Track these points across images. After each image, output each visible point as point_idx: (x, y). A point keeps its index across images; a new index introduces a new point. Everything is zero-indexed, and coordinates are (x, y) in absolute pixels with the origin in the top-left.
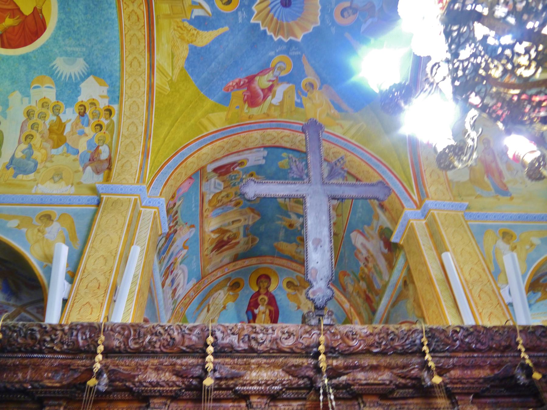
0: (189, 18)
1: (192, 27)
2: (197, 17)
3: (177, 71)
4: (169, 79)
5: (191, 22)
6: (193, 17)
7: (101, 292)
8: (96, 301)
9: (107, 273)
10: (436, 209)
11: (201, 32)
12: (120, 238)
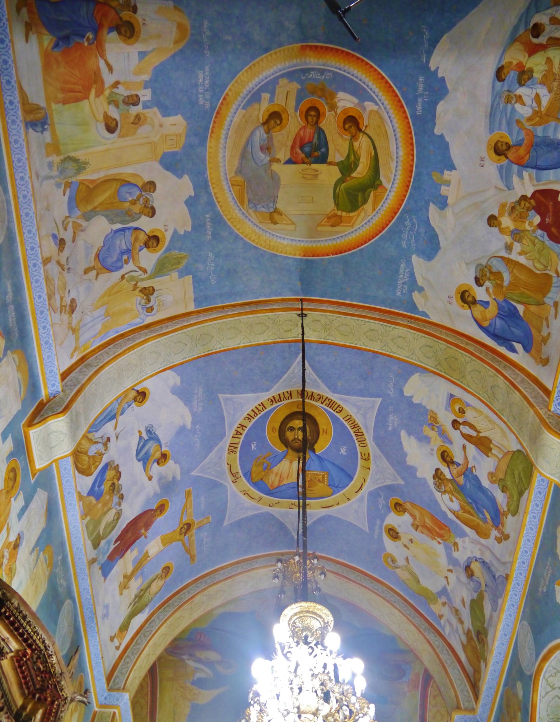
5: (193, 683)
6: (195, 679)
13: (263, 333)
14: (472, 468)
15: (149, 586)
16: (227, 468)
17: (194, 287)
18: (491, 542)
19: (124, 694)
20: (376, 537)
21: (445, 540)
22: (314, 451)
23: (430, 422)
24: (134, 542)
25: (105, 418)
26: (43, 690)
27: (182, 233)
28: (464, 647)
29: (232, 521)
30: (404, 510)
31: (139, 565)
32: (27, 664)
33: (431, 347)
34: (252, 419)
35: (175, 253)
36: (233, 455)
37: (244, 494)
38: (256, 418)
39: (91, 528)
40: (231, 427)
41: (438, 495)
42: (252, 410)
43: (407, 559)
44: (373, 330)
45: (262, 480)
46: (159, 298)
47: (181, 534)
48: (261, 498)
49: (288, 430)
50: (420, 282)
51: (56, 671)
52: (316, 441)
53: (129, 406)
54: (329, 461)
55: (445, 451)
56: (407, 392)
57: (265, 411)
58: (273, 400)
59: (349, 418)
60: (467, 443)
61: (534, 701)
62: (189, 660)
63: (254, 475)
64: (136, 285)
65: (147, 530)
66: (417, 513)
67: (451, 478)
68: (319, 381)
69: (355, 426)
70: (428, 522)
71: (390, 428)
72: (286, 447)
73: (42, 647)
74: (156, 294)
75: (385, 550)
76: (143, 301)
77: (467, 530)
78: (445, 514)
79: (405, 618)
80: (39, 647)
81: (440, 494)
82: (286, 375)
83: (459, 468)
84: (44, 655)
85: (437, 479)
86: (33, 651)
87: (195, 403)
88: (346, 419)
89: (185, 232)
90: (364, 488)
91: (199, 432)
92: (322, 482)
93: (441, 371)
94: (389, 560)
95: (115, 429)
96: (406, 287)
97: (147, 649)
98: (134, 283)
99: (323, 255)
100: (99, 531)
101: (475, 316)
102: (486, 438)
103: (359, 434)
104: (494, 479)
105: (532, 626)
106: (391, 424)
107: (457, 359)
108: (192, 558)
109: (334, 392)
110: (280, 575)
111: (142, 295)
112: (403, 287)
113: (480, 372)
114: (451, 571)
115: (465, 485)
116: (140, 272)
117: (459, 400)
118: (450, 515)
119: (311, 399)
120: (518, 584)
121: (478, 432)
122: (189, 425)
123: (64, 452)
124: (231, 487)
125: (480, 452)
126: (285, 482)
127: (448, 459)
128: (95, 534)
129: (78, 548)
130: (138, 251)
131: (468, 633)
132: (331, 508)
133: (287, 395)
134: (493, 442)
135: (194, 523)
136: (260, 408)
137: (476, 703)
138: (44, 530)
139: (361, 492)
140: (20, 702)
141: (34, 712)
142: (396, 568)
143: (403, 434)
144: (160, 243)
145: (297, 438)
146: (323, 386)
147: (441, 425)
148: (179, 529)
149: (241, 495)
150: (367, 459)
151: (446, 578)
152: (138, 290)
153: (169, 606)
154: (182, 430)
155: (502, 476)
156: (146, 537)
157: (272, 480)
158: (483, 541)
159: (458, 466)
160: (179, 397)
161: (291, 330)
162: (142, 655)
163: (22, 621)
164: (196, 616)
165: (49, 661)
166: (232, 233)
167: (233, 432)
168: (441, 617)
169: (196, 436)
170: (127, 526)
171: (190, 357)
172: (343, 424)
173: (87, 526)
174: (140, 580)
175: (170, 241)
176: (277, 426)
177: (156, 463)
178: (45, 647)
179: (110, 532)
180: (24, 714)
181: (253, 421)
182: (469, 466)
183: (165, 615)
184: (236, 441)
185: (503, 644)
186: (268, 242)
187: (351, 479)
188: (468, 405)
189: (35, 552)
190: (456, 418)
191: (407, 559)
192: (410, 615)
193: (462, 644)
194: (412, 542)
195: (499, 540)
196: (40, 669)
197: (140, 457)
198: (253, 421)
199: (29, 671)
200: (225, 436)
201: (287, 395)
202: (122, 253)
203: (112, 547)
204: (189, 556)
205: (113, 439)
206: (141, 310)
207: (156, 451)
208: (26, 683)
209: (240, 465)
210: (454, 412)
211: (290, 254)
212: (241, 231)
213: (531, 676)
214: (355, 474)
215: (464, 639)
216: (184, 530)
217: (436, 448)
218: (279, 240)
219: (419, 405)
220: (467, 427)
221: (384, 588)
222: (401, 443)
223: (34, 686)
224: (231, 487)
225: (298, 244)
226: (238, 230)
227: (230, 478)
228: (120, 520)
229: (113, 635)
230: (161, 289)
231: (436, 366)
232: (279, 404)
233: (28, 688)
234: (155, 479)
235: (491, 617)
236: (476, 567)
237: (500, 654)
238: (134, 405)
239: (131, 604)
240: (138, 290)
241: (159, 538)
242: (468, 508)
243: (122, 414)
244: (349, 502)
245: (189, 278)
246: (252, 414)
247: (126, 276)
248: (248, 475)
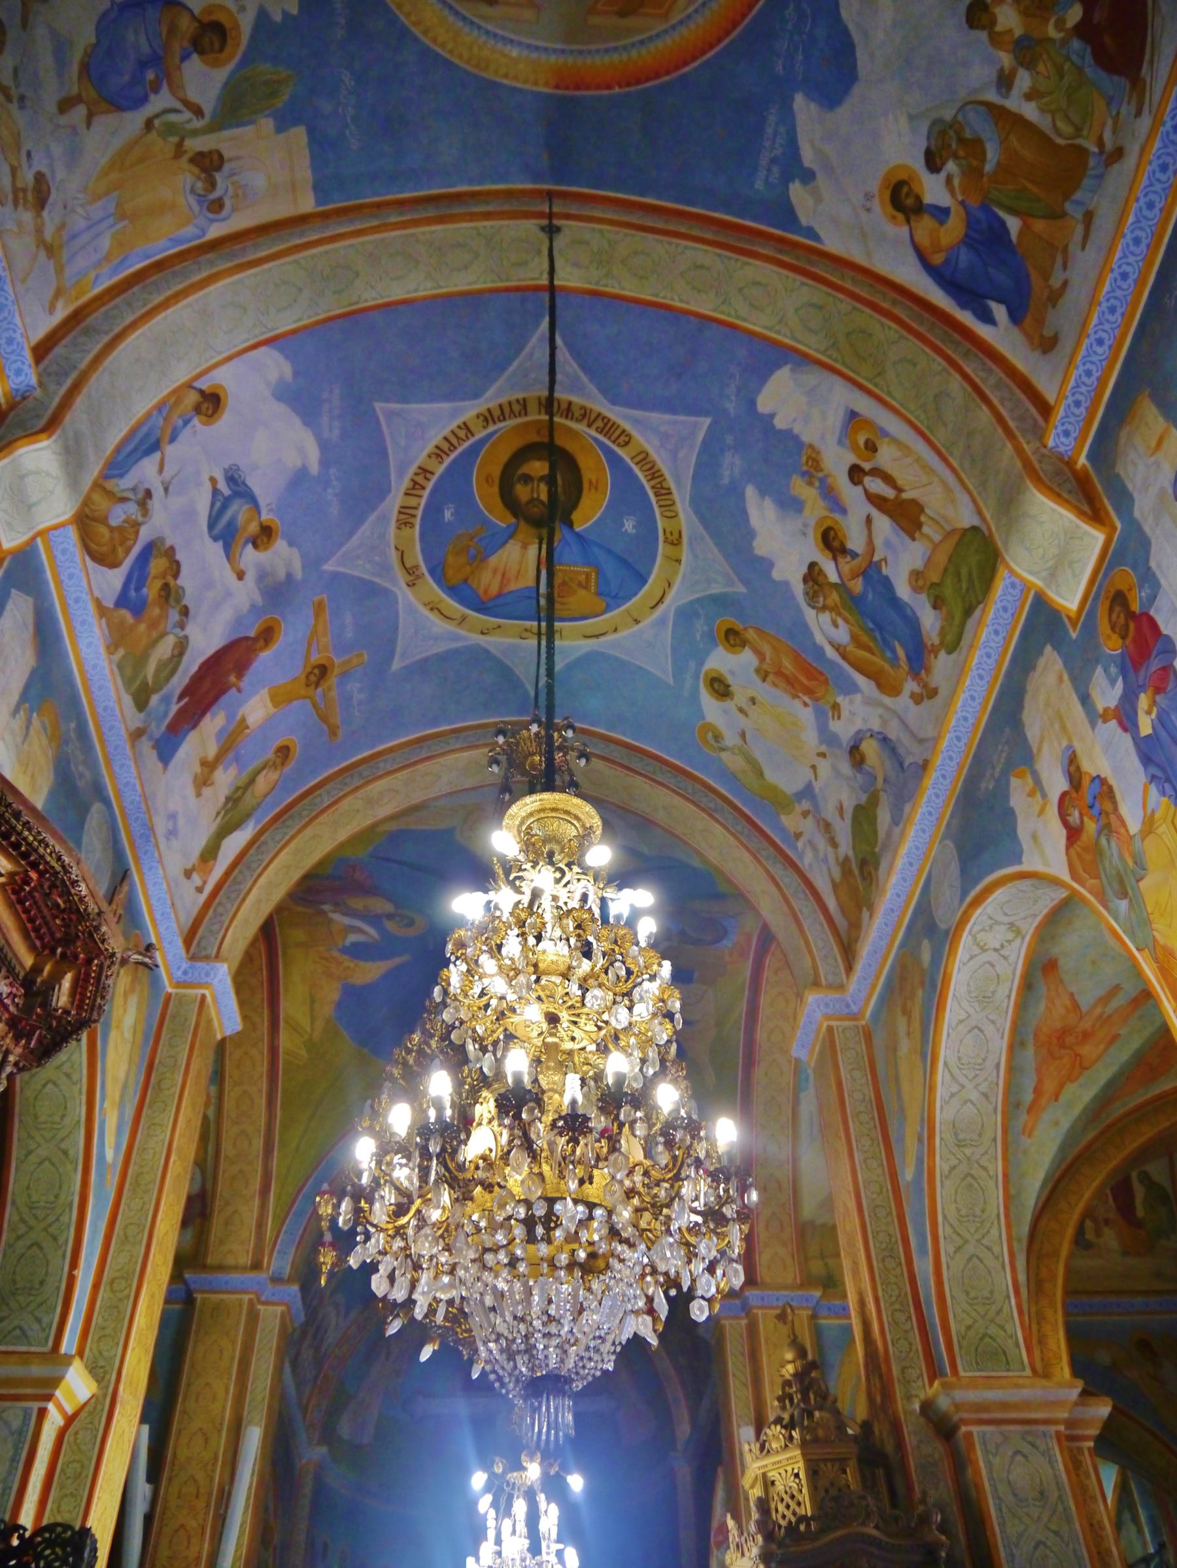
0: (340, 946)
1: (345, 957)
2: (355, 945)
3: (320, 1024)
4: (306, 1037)
5: (345, 950)
7: (201, 1504)
8: (194, 1524)
9: (210, 1467)
10: (763, 1307)
11: (362, 963)
12: (227, 1390)
13: (466, 268)
14: (880, 561)
15: (252, 781)
16: (394, 556)
17: (313, 157)
18: (903, 701)
19: (218, 965)
20: (686, 694)
21: (817, 700)
22: (570, 525)
23: (805, 468)
24: (216, 699)
25: (135, 450)
26: (67, 941)
27: (278, 18)
28: (835, 886)
29: (408, 662)
30: (744, 643)
31: (229, 744)
32: (33, 897)
33: (820, 308)
34: (444, 456)
35: (265, 69)
36: (406, 531)
37: (432, 609)
38: (453, 456)
39: (129, 671)
40: (401, 472)
41: (810, 614)
42: (446, 439)
43: (743, 735)
44: (702, 267)
45: (466, 581)
46: (236, 178)
47: (307, 685)
48: (464, 618)
49: (519, 480)
50: (808, 157)
51: (90, 909)
52: (574, 506)
53: (186, 423)
54: (600, 546)
56: (764, 403)
57: (472, 440)
58: (488, 418)
59: (644, 459)
60: (875, 513)
61: (949, 971)
62: (334, 912)
63: (450, 572)
64: (180, 145)
65: (240, 676)
66: (767, 649)
68: (584, 378)
69: (654, 474)
70: (788, 665)
71: (726, 481)
72: (515, 516)
73: (58, 868)
74: (227, 167)
75: (703, 718)
76: (199, 185)
77: (861, 680)
78: (820, 651)
79: (731, 838)
80: (53, 868)
82: (515, 364)
83: (855, 562)
84: (63, 881)
85: (811, 583)
86: (41, 874)
87: (325, 420)
88: (637, 459)
89: (285, 14)
90: (668, 600)
91: (335, 483)
92: (586, 587)
93: (836, 360)
94: (710, 735)
95: (161, 470)
96: (776, 170)
97: (255, 891)
98: (174, 139)
99: (598, 87)
100: (145, 677)
101: (916, 239)
102: (914, 502)
103: (664, 492)
104: (920, 583)
105: (960, 848)
106: (727, 473)
107: (870, 335)
108: (333, 732)
109: (614, 401)
110: (503, 758)
111: (196, 170)
112: (769, 170)
113: (915, 365)
114: (822, 755)
116: (188, 115)
117: (868, 424)
118: (830, 653)
119: (567, 417)
120: (944, 776)
121: (900, 490)
122: (314, 468)
123: (58, 516)
124: (404, 594)
126: (513, 586)
127: (836, 544)
128: (138, 682)
129: (105, 709)
130: (177, 60)
131: (845, 863)
132: (602, 639)
133: (516, 408)
134: (927, 511)
135: (333, 664)
136: (462, 434)
137: (848, 976)
138: (33, 673)
139: (661, 608)
140: (28, 961)
141: (56, 978)
142: (723, 749)
143: (750, 492)
144: (229, 41)
145: (538, 500)
146: (592, 388)
147: (826, 476)
148: (303, 677)
149: (425, 612)
150: (675, 541)
151: (814, 767)
152: (186, 157)
153: (291, 817)
154: (300, 477)
155: (935, 578)
156: (239, 690)
157: (487, 581)
158: (887, 700)
159: (853, 559)
160: (294, 409)
161: (525, 263)
162: (247, 902)
163: (13, 821)
164: (343, 835)
165: (73, 891)
166: (393, 21)
167: (406, 483)
168: (798, 836)
169: (330, 491)
170: (200, 668)
171: (309, 317)
172: (630, 470)
173: (120, 667)
174: (232, 771)
175: (253, 37)
176: (496, 471)
177: (250, 546)
178: (63, 867)
179: (168, 679)
180: (39, 980)
181: (448, 461)
182: (876, 558)
183: (286, 834)
184: (412, 501)
185: (905, 880)
186: (475, 50)
187: (643, 581)
188: (885, 434)
189: (22, 713)
190: (858, 462)
191: (743, 735)
192: (742, 833)
193: (833, 881)
194: (754, 703)
195: (917, 699)
196: (58, 905)
197: (216, 531)
198: (448, 461)
199: (38, 908)
200: (389, 491)
201: (516, 408)
202: (143, 65)
203: (174, 708)
204: (325, 727)
205: (158, 493)
206: (196, 208)
207: (249, 521)
208: (37, 930)
209: (423, 551)
210: (854, 448)
211: (526, 81)
212: (413, 18)
213: (947, 933)
214: (649, 573)
215: (837, 874)
216: (313, 678)
217: (812, 523)
218: (500, 45)
219: (789, 436)
220: (879, 481)
221: (698, 787)
223: (52, 934)
224: (404, 594)
225: (544, 57)
226: (408, 15)
227: (401, 578)
228: (186, 658)
229: (189, 866)
230: (238, 158)
231: (827, 349)
232: (500, 425)
233: (41, 938)
234: (250, 577)
235: (889, 835)
236: (870, 748)
237: (898, 895)
238: (196, 421)
239: (218, 813)
240: (186, 157)
241: (264, 693)
242: (865, 639)
243: (172, 439)
244: (636, 628)
245: (299, 134)
246: (445, 446)
247: (157, 122)
248: (438, 572)
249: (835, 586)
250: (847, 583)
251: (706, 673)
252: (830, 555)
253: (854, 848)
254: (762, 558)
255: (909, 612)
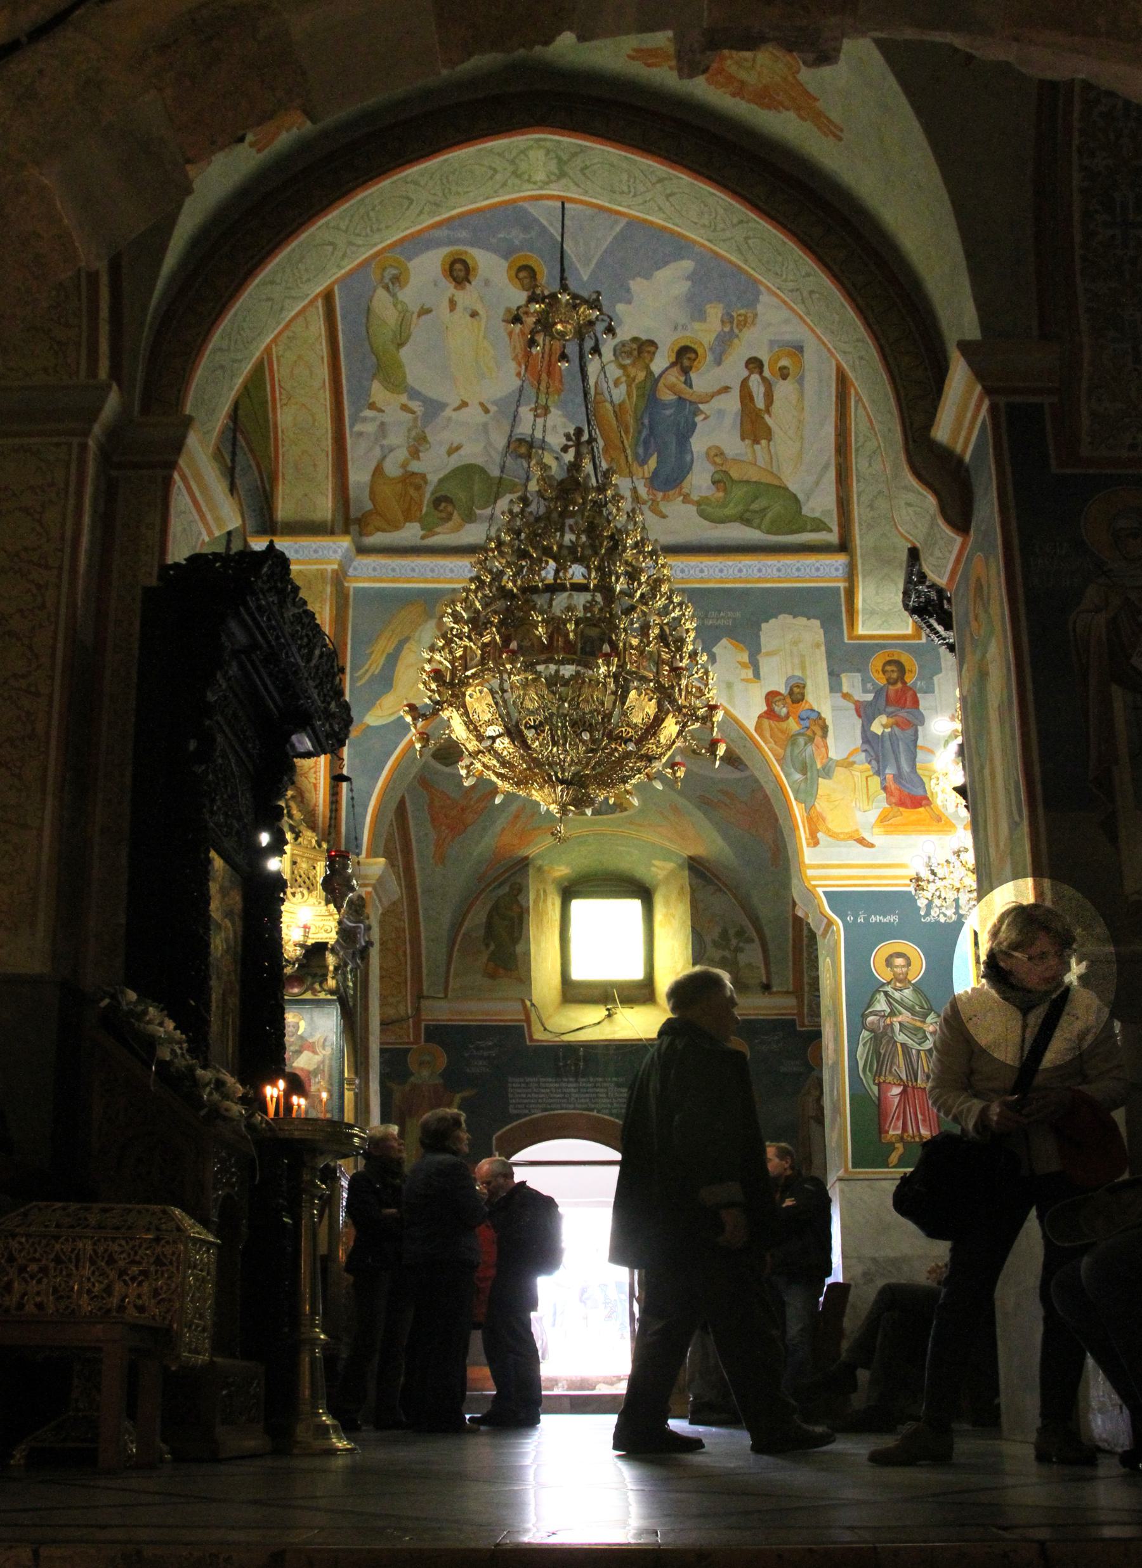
14: (702, 412)
23: (734, 314)
55: (695, 352)
60: (736, 393)
67: (656, 376)
81: (613, 358)
83: (683, 386)
85: (635, 346)
102: (769, 429)
104: (718, 460)
115: (665, 406)
121: (768, 411)
125: (739, 422)
127: (686, 363)
134: (771, 443)
143: (688, 265)
147: (737, 336)
159: (685, 383)
182: (701, 406)
188: (801, 381)
220: (762, 389)
222: (666, 263)
249: (650, 373)
250: (661, 384)
251: (466, 253)
252: (673, 359)
253: (441, 481)
254: (628, 290)
255: (688, 458)
